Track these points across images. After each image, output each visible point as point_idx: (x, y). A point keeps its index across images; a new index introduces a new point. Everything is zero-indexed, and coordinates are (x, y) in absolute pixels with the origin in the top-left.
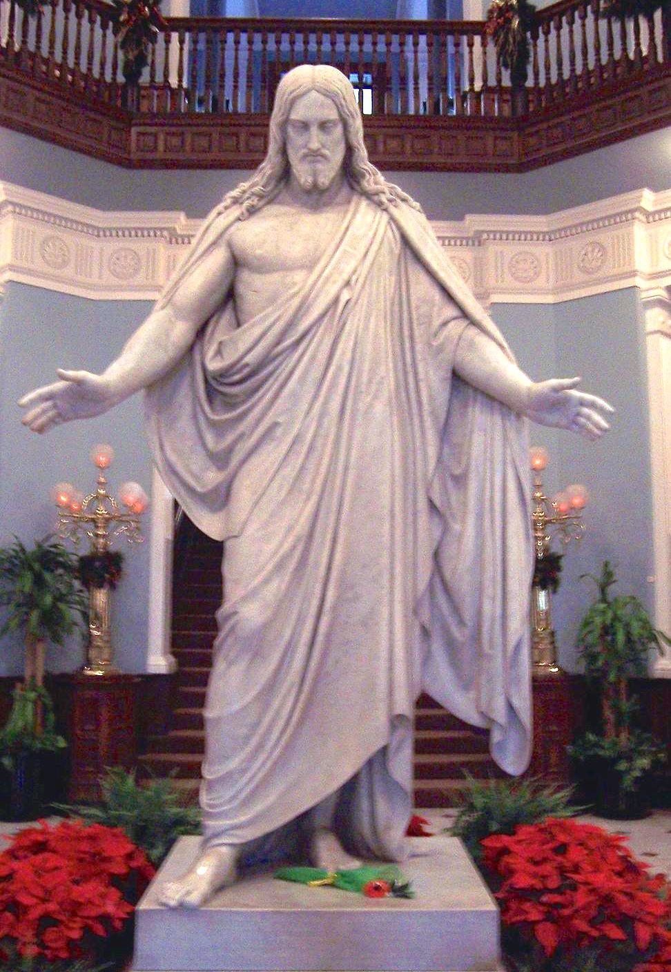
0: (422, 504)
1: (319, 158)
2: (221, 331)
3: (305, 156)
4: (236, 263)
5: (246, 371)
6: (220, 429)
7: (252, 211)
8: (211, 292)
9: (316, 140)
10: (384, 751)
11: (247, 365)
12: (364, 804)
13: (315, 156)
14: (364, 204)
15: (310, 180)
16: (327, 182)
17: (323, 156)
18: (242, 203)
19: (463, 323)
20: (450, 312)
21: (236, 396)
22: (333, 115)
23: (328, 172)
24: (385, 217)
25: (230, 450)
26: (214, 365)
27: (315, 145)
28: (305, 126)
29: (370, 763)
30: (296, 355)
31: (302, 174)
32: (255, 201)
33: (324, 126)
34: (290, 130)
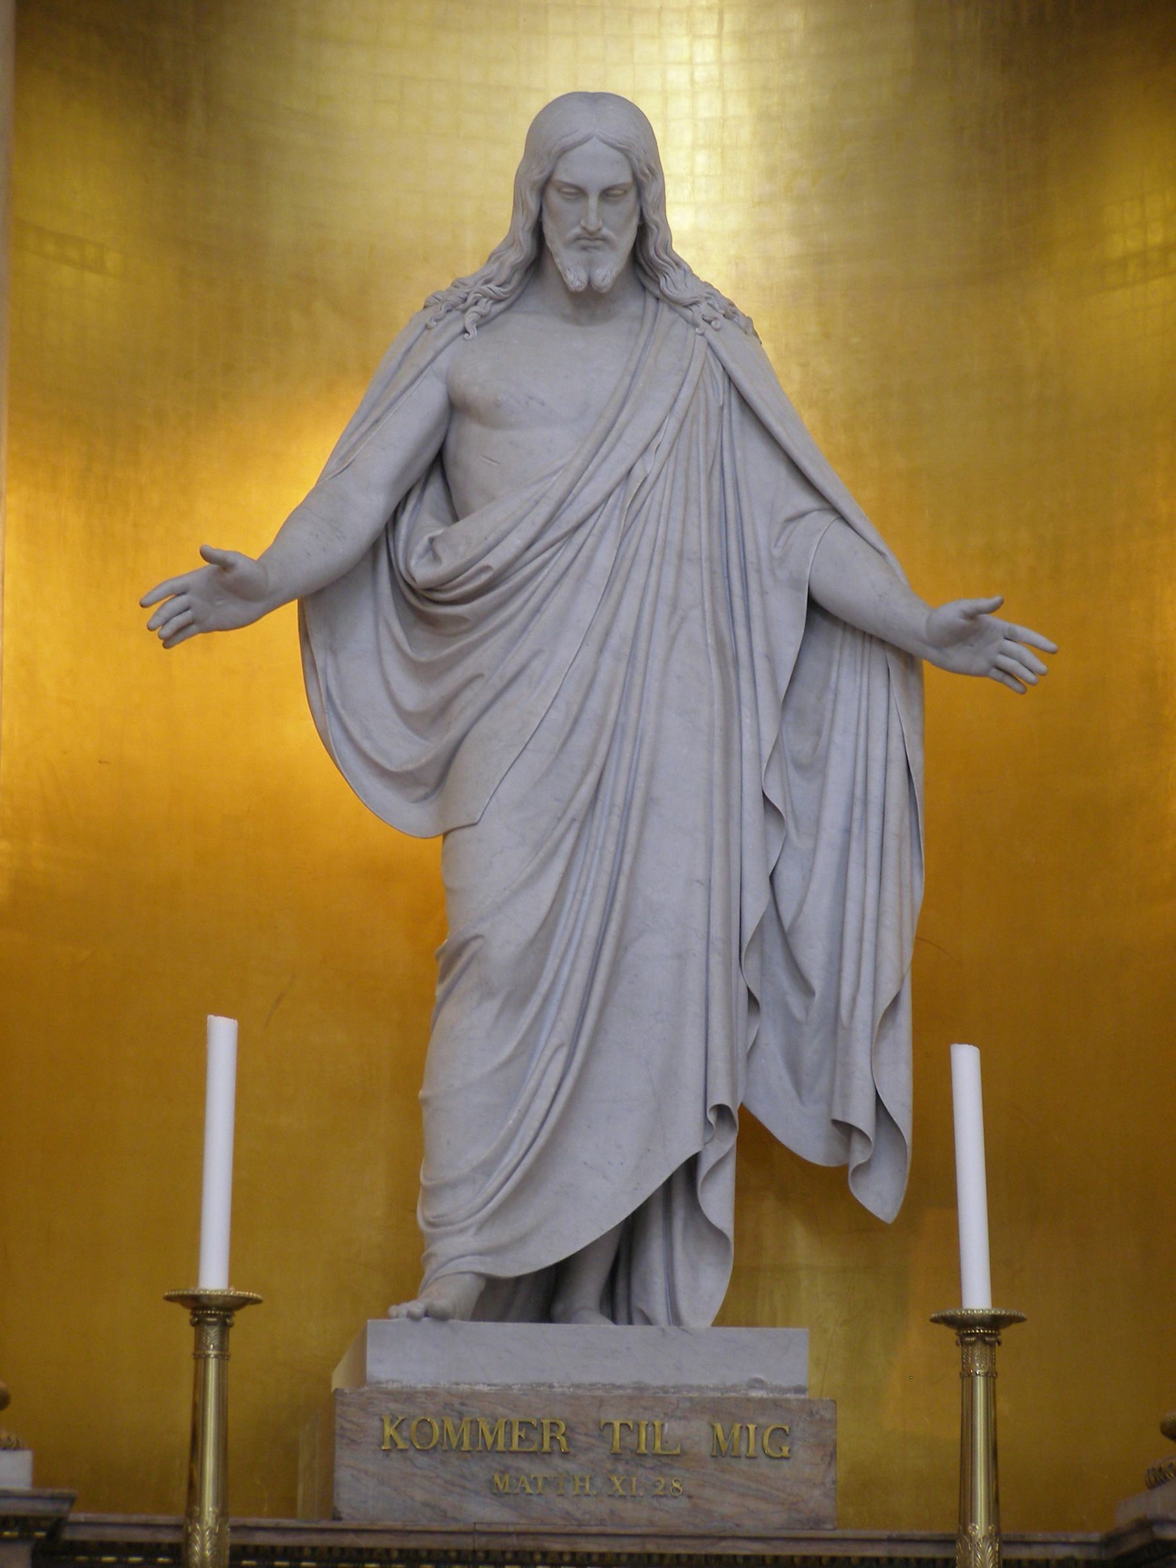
0: (752, 809)
1: (599, 243)
2: (423, 522)
3: (578, 238)
4: (455, 409)
5: (484, 577)
6: (424, 672)
7: (484, 322)
8: (416, 455)
9: (593, 212)
10: (692, 1165)
11: (487, 568)
12: (658, 1283)
13: (590, 240)
14: (666, 314)
15: (583, 277)
16: (609, 281)
17: (604, 239)
18: (464, 311)
19: (828, 520)
20: (805, 501)
21: (459, 620)
22: (625, 178)
23: (609, 268)
24: (701, 344)
25: (441, 711)
26: (423, 572)
27: (593, 223)
28: (580, 192)
29: (668, 1184)
30: (569, 553)
31: (572, 269)
32: (484, 306)
33: (606, 194)
34: (554, 197)
